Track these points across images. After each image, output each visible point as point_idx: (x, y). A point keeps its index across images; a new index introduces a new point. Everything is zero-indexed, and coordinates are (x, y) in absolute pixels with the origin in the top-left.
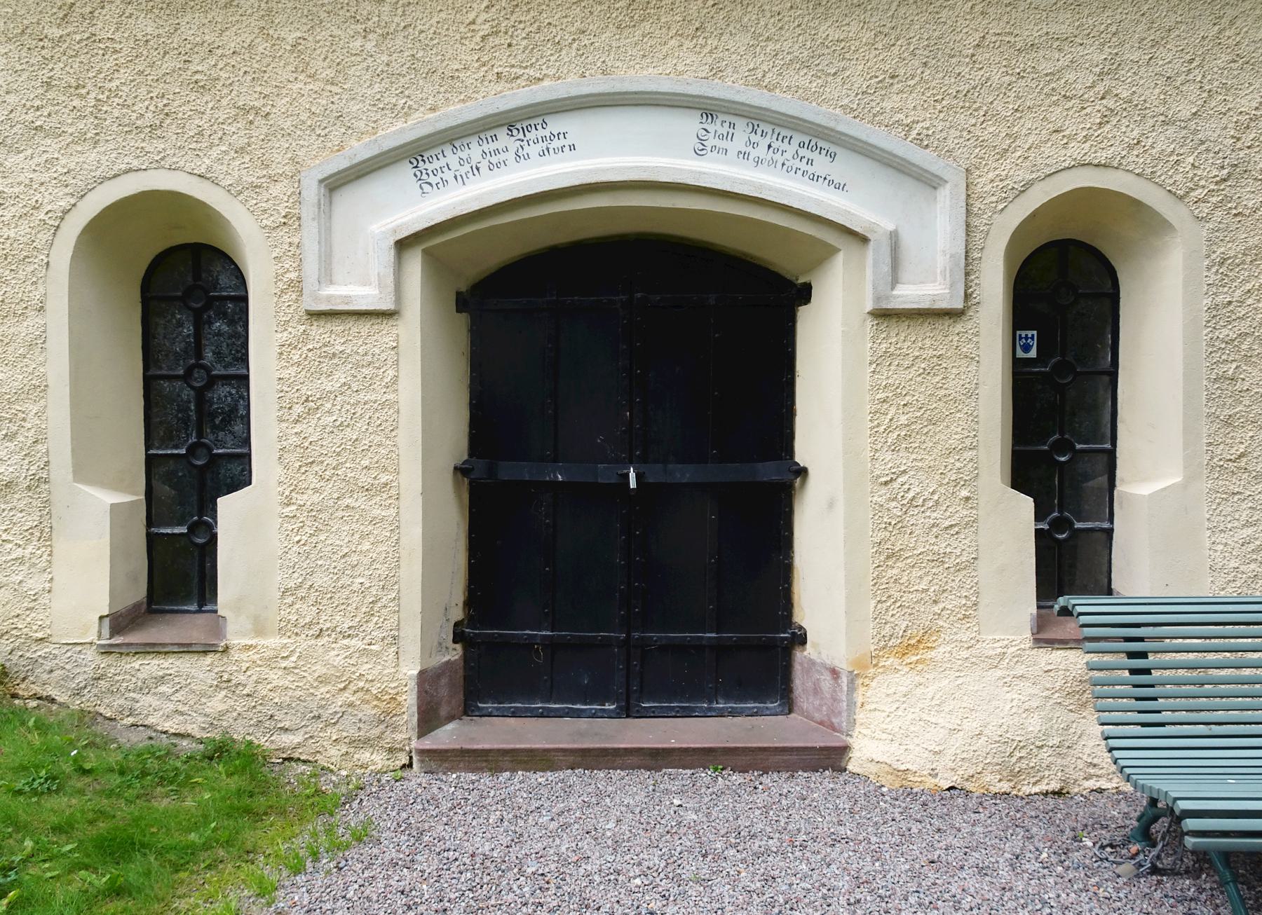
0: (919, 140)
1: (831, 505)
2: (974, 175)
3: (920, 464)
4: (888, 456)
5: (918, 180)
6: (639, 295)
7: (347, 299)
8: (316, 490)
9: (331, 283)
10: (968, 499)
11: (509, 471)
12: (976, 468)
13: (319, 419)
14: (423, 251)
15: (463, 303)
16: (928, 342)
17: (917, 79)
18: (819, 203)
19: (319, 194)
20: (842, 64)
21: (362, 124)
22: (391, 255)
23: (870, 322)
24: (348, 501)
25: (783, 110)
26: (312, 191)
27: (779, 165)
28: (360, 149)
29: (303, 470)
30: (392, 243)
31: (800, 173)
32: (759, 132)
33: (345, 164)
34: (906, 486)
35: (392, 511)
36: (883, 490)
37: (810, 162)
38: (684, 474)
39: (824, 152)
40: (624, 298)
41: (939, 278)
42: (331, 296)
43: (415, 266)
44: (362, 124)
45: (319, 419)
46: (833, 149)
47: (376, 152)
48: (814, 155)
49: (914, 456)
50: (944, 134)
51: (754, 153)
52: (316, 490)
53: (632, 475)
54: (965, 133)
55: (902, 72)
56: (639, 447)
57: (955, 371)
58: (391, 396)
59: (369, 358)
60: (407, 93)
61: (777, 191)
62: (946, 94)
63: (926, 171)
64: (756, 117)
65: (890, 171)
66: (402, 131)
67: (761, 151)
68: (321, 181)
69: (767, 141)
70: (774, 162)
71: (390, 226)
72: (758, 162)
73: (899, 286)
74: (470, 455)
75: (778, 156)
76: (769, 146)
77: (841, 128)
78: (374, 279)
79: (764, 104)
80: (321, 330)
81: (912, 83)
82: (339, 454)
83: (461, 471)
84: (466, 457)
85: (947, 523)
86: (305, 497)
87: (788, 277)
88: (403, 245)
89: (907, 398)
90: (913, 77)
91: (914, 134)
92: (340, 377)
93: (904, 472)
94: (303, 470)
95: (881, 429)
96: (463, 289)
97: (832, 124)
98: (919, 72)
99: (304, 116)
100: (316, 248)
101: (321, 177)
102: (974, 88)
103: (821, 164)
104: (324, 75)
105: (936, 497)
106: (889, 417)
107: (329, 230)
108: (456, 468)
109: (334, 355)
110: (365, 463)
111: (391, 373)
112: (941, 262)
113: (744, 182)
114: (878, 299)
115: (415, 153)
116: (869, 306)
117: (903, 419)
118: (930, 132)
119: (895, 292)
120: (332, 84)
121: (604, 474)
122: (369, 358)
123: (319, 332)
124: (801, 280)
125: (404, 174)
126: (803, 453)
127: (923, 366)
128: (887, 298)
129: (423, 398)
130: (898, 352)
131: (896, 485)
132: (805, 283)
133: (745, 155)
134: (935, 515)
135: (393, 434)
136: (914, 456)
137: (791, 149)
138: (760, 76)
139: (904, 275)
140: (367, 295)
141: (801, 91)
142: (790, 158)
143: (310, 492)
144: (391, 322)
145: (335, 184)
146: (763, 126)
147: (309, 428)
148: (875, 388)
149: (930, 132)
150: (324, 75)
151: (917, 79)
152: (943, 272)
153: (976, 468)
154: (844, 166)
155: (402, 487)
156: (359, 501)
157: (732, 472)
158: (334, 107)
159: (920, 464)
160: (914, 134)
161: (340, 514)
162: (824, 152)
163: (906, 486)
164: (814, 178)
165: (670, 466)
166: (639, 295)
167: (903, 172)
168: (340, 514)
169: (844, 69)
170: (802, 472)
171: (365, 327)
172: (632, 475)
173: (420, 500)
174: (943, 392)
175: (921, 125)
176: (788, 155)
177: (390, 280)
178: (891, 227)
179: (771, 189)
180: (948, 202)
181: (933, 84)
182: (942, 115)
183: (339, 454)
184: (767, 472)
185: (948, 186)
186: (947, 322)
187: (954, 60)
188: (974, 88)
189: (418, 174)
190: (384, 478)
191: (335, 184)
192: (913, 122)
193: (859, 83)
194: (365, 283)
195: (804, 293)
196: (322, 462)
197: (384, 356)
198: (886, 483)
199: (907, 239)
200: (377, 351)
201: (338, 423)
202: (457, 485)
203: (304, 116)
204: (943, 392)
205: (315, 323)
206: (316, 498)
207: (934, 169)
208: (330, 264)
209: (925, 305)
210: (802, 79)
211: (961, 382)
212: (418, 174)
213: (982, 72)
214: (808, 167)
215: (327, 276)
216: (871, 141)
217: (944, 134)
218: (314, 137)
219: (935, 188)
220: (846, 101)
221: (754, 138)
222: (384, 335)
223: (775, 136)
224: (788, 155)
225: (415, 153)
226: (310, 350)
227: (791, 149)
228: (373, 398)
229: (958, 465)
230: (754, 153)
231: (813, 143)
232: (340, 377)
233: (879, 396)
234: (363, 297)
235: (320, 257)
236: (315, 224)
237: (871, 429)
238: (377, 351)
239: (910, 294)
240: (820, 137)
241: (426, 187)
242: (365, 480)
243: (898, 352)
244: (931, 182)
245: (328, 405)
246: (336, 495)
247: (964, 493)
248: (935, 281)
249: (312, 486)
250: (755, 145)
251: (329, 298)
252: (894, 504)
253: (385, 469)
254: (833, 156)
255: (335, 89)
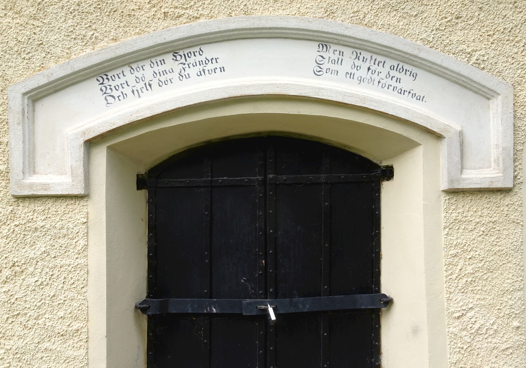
0: (477, 64)
1: (416, 331)
2: (517, 90)
3: (483, 302)
4: (460, 297)
5: (476, 92)
6: (271, 176)
7: (45, 186)
8: (20, 337)
9: (34, 172)
10: (518, 328)
11: (179, 305)
12: (523, 305)
13: (24, 280)
14: (108, 148)
15: (141, 183)
16: (485, 212)
17: (475, 19)
18: (407, 110)
19: (23, 105)
20: (421, 9)
21: (58, 50)
22: (80, 152)
23: (444, 198)
24: (47, 345)
25: (380, 41)
26: (16, 102)
27: (376, 82)
28: (56, 70)
29: (10, 320)
30: (82, 142)
31: (391, 88)
32: (361, 58)
33: (43, 81)
34: (473, 320)
35: (83, 352)
36: (457, 323)
37: (398, 80)
38: (305, 305)
39: (408, 73)
40: (260, 178)
41: (493, 165)
42: (34, 184)
43: (101, 157)
44: (58, 50)
45: (24, 280)
46: (415, 70)
47: (69, 71)
48: (401, 76)
49: (478, 296)
50: (495, 60)
51: (358, 74)
52: (20, 337)
53: (271, 311)
54: (510, 59)
55: (464, 14)
56: (272, 290)
57: (505, 232)
58: (82, 261)
59: (64, 231)
60: (94, 27)
61: (376, 101)
62: (496, 31)
63: (484, 87)
64: (359, 46)
65: (456, 87)
66: (89, 55)
67: (363, 72)
68: (25, 94)
69: (367, 65)
70: (372, 80)
71: (80, 130)
72: (361, 80)
73: (465, 171)
74: (148, 296)
75: (375, 76)
76: (369, 69)
77: (422, 55)
78: (69, 170)
79: (366, 37)
80: (26, 210)
81: (471, 22)
82: (39, 308)
83: (141, 308)
84: (145, 295)
85: (504, 346)
86: (12, 342)
87: (375, 161)
88: (91, 144)
89: (472, 253)
90: (472, 18)
91: (474, 59)
92: (41, 246)
93: (472, 308)
94: (10, 320)
95: (454, 276)
96: (143, 172)
97: (416, 52)
98: (476, 14)
99: (12, 44)
100: (21, 146)
101: (24, 90)
102: (516, 26)
103: (407, 82)
104: (28, 12)
105: (495, 327)
106: (459, 267)
107: (32, 132)
108: (136, 307)
109: (36, 229)
110: (61, 314)
111: (82, 242)
112: (494, 153)
113: (352, 95)
114: (451, 181)
115: (100, 72)
116: (445, 186)
117: (469, 269)
118: (485, 58)
119: (463, 176)
120: (35, 19)
121: (248, 306)
122: (64, 231)
123: (24, 210)
124: (384, 164)
125: (93, 87)
126: (387, 287)
127: (482, 229)
128: (458, 180)
129: (108, 261)
130: (464, 219)
131: (465, 319)
132: (387, 167)
133: (351, 75)
134: (494, 340)
135: (84, 290)
136: (478, 296)
137: (385, 71)
138: (362, 16)
139: (468, 163)
140: (64, 182)
141: (392, 28)
142: (384, 77)
143: (16, 338)
144: (82, 203)
145: (36, 96)
146: (364, 54)
147: (16, 288)
148: (449, 246)
149: (485, 58)
150: (28, 12)
151: (475, 19)
152: (497, 161)
153: (523, 305)
154: (424, 83)
155: (90, 331)
156: (56, 345)
157: (340, 302)
158: (36, 37)
159: (483, 302)
160: (474, 59)
161: (39, 355)
162: (408, 73)
163: (473, 320)
164: (402, 92)
165: (295, 300)
166: (271, 176)
167: (466, 87)
168: (39, 355)
169: (423, 12)
170: (388, 302)
171: (61, 207)
172: (271, 311)
173: (105, 341)
174: (497, 248)
175: (479, 53)
176: (383, 75)
177: (81, 171)
178: (459, 129)
179: (372, 100)
180: (500, 109)
181: (487, 23)
182: (493, 46)
183: (39, 308)
184: (363, 301)
185: (500, 97)
186: (499, 196)
187: (501, 6)
188: (516, 26)
189: (104, 89)
190: (76, 325)
191: (36, 96)
192: (473, 51)
193: (435, 23)
194: (62, 173)
195: (388, 173)
196: (26, 314)
197: (76, 229)
198: (459, 317)
199: (469, 137)
200: (71, 226)
201: (39, 283)
202: (137, 319)
203: (12, 44)
204: (497, 248)
205: (21, 205)
206: (20, 343)
207: (489, 85)
208: (34, 158)
209: (485, 185)
210: (392, 19)
211: (510, 241)
212: (104, 89)
213: (522, 15)
214: (397, 85)
215: (30, 166)
216: (444, 65)
217: (495, 60)
218: (20, 60)
219: (488, 99)
220: (424, 36)
221: (358, 63)
222: (77, 212)
223: (373, 61)
224: (383, 75)
225: (100, 72)
226: (17, 226)
227: (385, 71)
228: (68, 262)
229: (510, 302)
230: (358, 74)
231: (400, 66)
232: (41, 246)
233: (451, 252)
234: (59, 184)
235: (24, 153)
236: (20, 127)
237: (447, 277)
238: (71, 226)
239: (475, 177)
240: (406, 61)
241: (110, 99)
242: (61, 327)
243: (464, 219)
244: (486, 94)
245: (31, 269)
246: (36, 341)
247: (516, 324)
248: (490, 167)
249: (17, 334)
250: (358, 68)
251: (31, 186)
252: (464, 333)
253: (76, 318)
254: (415, 76)
255: (36, 23)
